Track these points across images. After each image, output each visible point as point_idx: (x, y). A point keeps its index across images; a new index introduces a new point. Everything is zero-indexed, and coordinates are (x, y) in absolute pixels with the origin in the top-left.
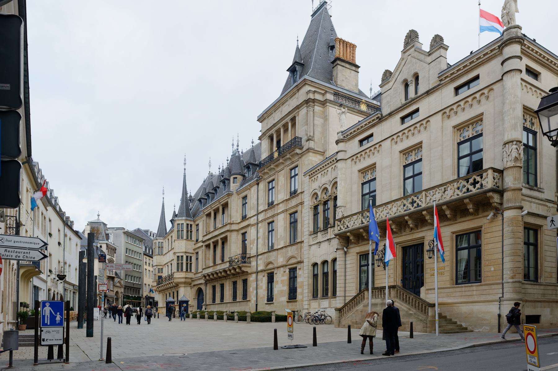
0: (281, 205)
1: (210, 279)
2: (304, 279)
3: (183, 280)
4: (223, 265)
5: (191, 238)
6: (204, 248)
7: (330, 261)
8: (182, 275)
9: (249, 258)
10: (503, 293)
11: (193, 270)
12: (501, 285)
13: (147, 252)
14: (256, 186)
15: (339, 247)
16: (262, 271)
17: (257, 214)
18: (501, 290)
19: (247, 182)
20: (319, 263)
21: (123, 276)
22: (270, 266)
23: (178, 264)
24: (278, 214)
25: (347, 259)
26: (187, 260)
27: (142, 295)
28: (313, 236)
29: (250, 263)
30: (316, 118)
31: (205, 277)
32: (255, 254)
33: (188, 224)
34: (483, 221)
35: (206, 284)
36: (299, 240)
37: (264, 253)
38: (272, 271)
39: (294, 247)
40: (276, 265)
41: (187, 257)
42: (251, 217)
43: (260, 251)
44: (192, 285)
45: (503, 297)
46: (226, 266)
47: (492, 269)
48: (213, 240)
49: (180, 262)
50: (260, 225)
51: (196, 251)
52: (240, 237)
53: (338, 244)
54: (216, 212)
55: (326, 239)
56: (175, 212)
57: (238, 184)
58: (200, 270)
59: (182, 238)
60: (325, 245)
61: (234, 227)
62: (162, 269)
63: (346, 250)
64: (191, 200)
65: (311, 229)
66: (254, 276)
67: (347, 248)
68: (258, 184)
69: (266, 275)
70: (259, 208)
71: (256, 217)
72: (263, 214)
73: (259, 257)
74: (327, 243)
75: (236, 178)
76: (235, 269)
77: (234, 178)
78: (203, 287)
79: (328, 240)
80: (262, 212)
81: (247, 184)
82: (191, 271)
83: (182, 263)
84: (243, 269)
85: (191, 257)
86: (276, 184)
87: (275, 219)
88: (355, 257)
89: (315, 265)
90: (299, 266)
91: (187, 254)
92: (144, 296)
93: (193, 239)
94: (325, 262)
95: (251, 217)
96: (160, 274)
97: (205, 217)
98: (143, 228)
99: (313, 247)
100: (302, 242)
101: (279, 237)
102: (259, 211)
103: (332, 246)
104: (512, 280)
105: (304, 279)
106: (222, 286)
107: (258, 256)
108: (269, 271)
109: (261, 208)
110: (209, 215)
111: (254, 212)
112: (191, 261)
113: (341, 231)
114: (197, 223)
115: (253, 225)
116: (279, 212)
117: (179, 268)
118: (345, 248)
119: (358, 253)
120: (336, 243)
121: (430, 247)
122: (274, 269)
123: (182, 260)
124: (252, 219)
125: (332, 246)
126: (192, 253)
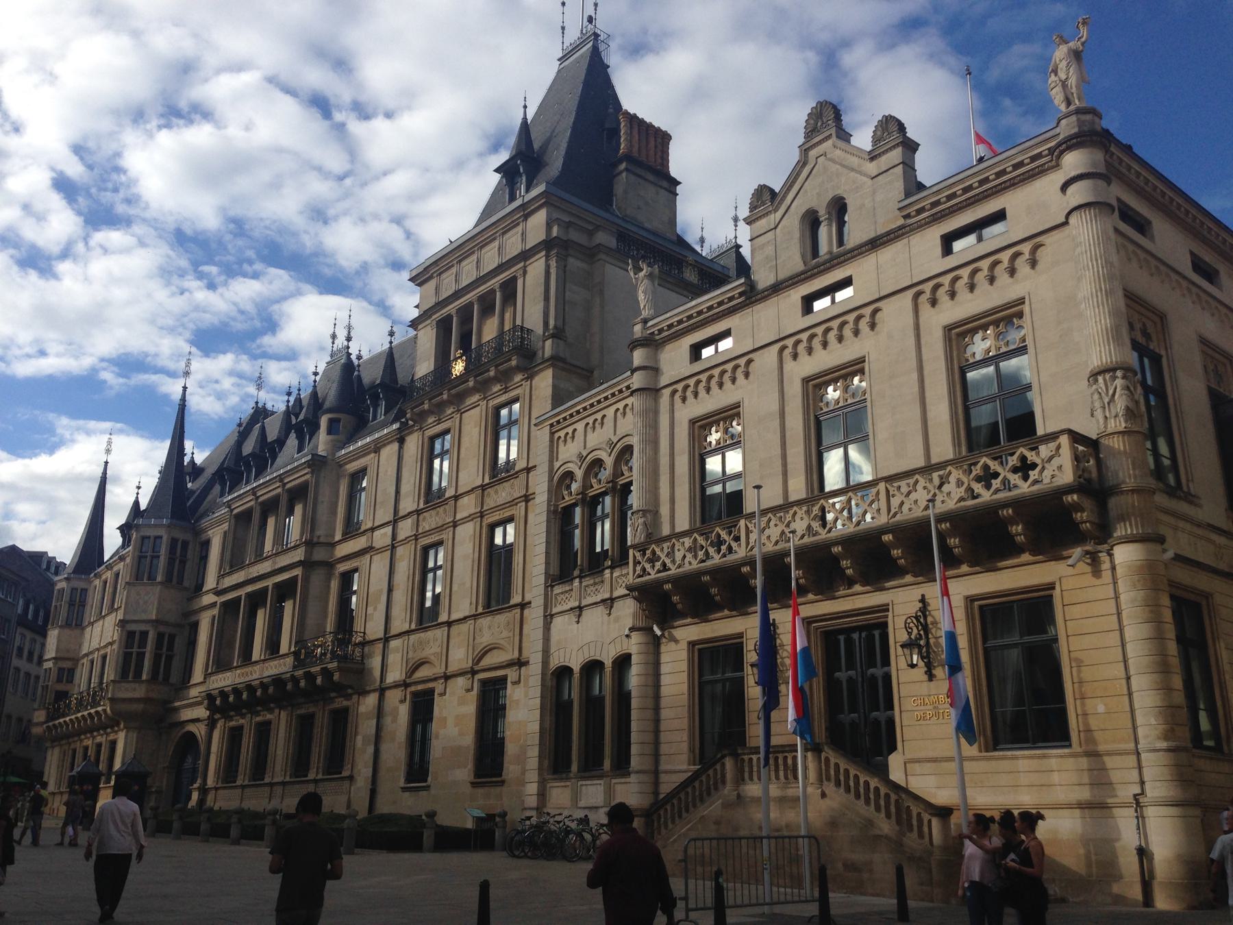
2: (524, 711)
3: (139, 707)
4: (273, 663)
5: (180, 581)
6: (215, 611)
7: (608, 663)
9: (364, 644)
10: (1142, 783)
11: (174, 678)
12: (1134, 757)
14: (396, 446)
15: (640, 624)
16: (396, 686)
17: (395, 522)
18: (1135, 775)
19: (370, 434)
20: (576, 667)
22: (422, 673)
23: (127, 657)
24: (455, 524)
25: (664, 658)
28: (558, 590)
30: (568, 285)
31: (210, 697)
32: (382, 635)
33: (173, 542)
34: (1065, 576)
36: (516, 599)
38: (431, 685)
39: (502, 619)
40: (439, 670)
41: (160, 636)
42: (373, 529)
45: (1143, 793)
47: (1101, 708)
48: (249, 589)
50: (400, 551)
51: (193, 619)
52: (335, 585)
53: (635, 616)
55: (599, 598)
56: (137, 503)
57: (342, 437)
58: (197, 676)
59: (152, 578)
60: (595, 617)
61: (319, 555)
62: (71, 672)
63: (659, 633)
64: (196, 471)
65: (554, 570)
66: (371, 700)
67: (662, 629)
68: (401, 441)
71: (389, 529)
72: (409, 521)
74: (601, 609)
75: (338, 420)
76: (310, 677)
77: (331, 421)
78: (200, 730)
79: (603, 601)
80: (409, 514)
81: (368, 440)
83: (141, 656)
84: (336, 677)
85: (172, 638)
86: (452, 445)
87: (446, 535)
88: (684, 655)
89: (564, 672)
90: (511, 674)
91: (162, 629)
93: (186, 584)
94: (593, 667)
99: (558, 622)
100: (523, 606)
102: (401, 513)
103: (617, 620)
104: (1164, 745)
105: (524, 711)
106: (264, 731)
107: (386, 639)
108: (420, 687)
109: (407, 505)
110: (243, 519)
111: (385, 515)
112: (171, 647)
113: (648, 578)
114: (204, 537)
116: (458, 517)
117: (129, 666)
118: (655, 628)
119: (692, 644)
120: (627, 610)
121: (910, 634)
122: (435, 679)
123: (143, 644)
124: (377, 533)
125: (617, 620)
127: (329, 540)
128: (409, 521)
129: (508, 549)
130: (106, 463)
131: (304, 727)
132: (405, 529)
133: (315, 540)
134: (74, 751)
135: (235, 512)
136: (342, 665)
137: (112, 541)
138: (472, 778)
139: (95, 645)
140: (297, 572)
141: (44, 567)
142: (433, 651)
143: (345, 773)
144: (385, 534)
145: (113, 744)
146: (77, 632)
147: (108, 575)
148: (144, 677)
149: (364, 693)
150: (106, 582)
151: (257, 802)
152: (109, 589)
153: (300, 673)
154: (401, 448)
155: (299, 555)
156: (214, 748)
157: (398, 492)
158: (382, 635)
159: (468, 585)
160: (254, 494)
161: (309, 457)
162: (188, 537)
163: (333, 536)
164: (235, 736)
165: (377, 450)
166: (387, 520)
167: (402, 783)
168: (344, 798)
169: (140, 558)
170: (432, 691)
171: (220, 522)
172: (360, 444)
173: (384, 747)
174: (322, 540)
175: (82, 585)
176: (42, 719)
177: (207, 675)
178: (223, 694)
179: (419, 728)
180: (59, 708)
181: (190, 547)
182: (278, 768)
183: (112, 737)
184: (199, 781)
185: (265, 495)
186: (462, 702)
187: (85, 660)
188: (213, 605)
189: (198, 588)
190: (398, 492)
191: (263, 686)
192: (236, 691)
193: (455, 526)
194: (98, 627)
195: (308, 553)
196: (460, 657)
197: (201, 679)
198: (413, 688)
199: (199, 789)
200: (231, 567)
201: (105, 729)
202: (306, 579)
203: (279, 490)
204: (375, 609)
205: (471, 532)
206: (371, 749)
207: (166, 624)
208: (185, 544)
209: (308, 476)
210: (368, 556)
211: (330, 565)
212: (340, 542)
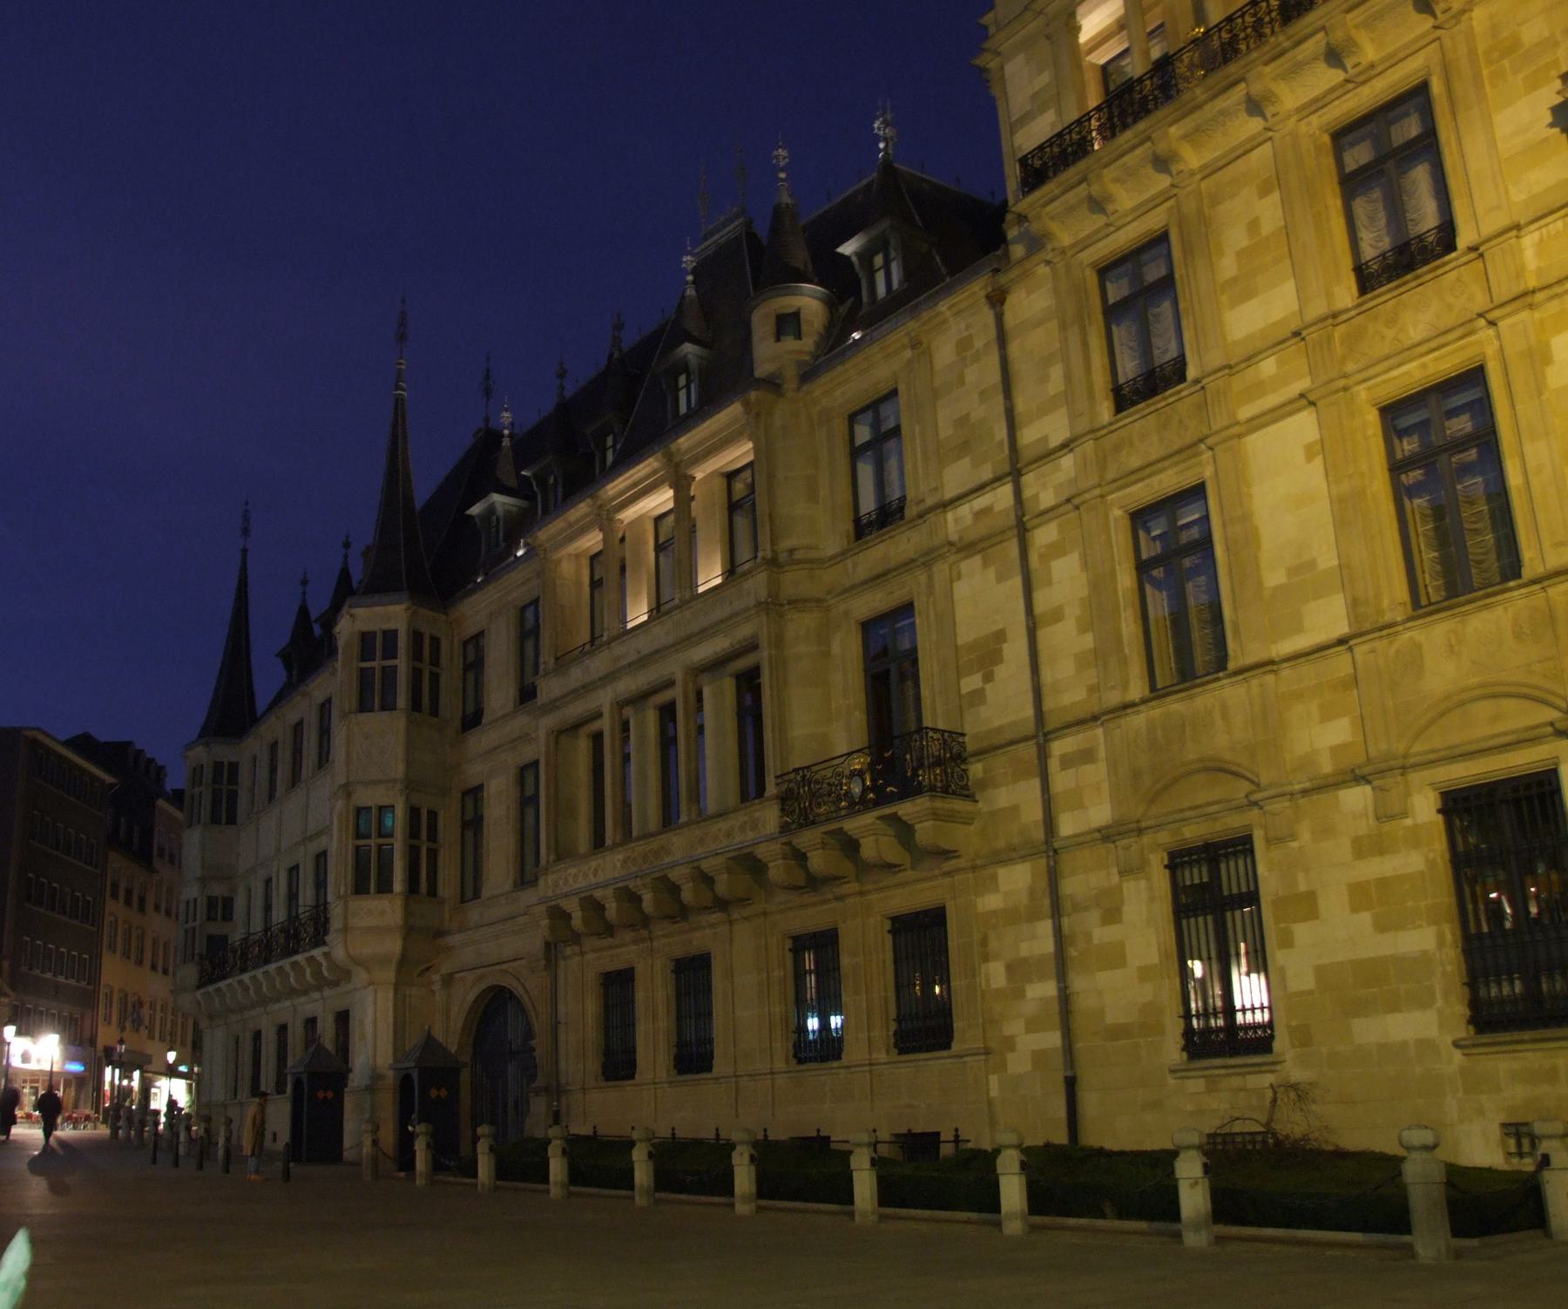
17: (1015, 472)
29: (966, 792)
41: (414, 813)
42: (945, 505)
49: (373, 842)
50: (1044, 536)
62: (228, 903)
66: (1018, 879)
70: (1028, 436)
71: (1005, 493)
78: (529, 986)
80: (1066, 446)
85: (433, 815)
96: (216, 929)
101: (1274, 578)
127: (814, 554)
128: (1067, 462)
130: (245, 551)
132: (1043, 489)
134: (257, 1035)
137: (267, 676)
138: (1463, 1031)
144: (986, 511)
148: (398, 886)
153: (806, 839)
154: (999, 319)
158: (1030, 728)
159: (1327, 559)
166: (986, 473)
174: (799, 555)
184: (540, 1081)
186: (1368, 847)
188: (524, 738)
196: (1323, 737)
198: (1164, 837)
201: (319, 988)
204: (988, 678)
205: (1312, 434)
206: (1049, 989)
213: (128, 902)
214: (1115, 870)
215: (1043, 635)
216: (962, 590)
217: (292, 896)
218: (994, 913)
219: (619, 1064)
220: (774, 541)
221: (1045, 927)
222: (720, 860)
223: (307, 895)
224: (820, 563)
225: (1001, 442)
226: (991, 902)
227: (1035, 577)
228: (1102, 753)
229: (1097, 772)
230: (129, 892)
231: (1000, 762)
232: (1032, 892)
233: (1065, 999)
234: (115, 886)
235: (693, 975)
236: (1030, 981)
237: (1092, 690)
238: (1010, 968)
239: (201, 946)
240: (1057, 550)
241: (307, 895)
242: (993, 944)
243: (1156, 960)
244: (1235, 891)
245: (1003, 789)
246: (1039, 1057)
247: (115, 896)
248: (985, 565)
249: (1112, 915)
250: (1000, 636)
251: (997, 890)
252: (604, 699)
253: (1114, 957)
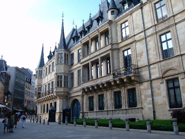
0: (179, 15)
1: (85, 91)
6: (81, 68)
8: (62, 90)
9: (138, 68)
11: (69, 86)
13: (27, 80)
14: (140, 10)
21: (13, 94)
23: (58, 82)
24: (176, 24)
26: (65, 79)
27: (23, 106)
31: (84, 89)
32: (147, 64)
33: (65, 54)
35: (83, 96)
37: (160, 61)
41: (65, 76)
42: (135, 36)
43: (152, 60)
44: (68, 97)
46: (110, 78)
49: (60, 80)
50: (148, 39)
51: (72, 72)
54: (96, 39)
56: (56, 46)
57: (115, 15)
61: (115, 47)
66: (146, 85)
68: (142, 8)
69: (165, 81)
71: (143, 34)
73: (152, 67)
76: (121, 80)
78: (79, 99)
80: (151, 27)
82: (67, 86)
83: (61, 81)
84: (133, 78)
85: (67, 77)
87: (170, 29)
91: (65, 75)
92: (24, 106)
93: (69, 64)
95: (135, 36)
96: (39, 92)
97: (82, 45)
98: (25, 68)
102: (146, 28)
107: (149, 65)
108: (170, 78)
109: (148, 25)
114: (72, 52)
115: (139, 41)
117: (59, 84)
123: (61, 78)
126: (69, 74)
128: (151, 29)
129: (129, 56)
131: (117, 95)
132: (149, 33)
133: (113, 43)
135: (82, 43)
136: (134, 74)
137: (46, 60)
139: (45, 82)
140: (110, 52)
141: (28, 71)
142: (174, 65)
143: (139, 106)
144: (140, 36)
145: (55, 103)
146: (41, 79)
147: (48, 66)
148: (63, 86)
149: (141, 83)
150: (47, 68)
151: (102, 116)
152: (48, 69)
153: (117, 79)
154: (142, 11)
155: (109, 47)
156: (84, 102)
157: (144, 23)
158: (147, 64)
160: (89, 37)
161: (108, 21)
162: (68, 53)
163: (117, 41)
164: (91, 99)
165: (131, 14)
167: (169, 109)
168: (141, 114)
169: (58, 58)
170: (177, 78)
171: (76, 48)
172: (121, 16)
173: (155, 98)
174: (115, 43)
175: (41, 70)
176: (36, 98)
177: (79, 85)
178: (88, 88)
179: (172, 91)
180: (40, 96)
181: (69, 55)
182: (109, 106)
183: (55, 101)
184: (81, 111)
185: (92, 36)
187: (44, 85)
189: (72, 64)
190: (144, 23)
191: (103, 84)
192: (93, 87)
193: (175, 25)
194: (46, 78)
195: (112, 47)
197: (77, 86)
198: (166, 79)
199: (82, 113)
200: (83, 57)
202: (112, 54)
203: (98, 33)
206: (151, 99)
207: (66, 74)
208: (67, 55)
209: (108, 26)
210: (134, 44)
211: (119, 49)
212: (121, 42)
213: (28, 88)
214: (159, 83)
215: (149, 52)
216: (137, 46)
217: (49, 87)
218: (142, 89)
219: (91, 109)
220: (112, 40)
221: (150, 91)
222: (105, 82)
223: (51, 87)
224: (118, 44)
225: (142, 27)
226: (142, 87)
227: (148, 44)
228: (157, 67)
229: (157, 70)
230: (28, 87)
231: (143, 69)
232: (147, 85)
233: (153, 100)
234: (26, 87)
235: (101, 97)
236: (147, 98)
237: (155, 59)
238: (145, 96)
239: (37, 94)
240: (150, 41)
241: (51, 87)
242: (142, 93)
243: (165, 95)
244: (178, 85)
245: (143, 72)
246: (149, 108)
247: (26, 87)
248: (140, 43)
249: (159, 89)
250: (142, 52)
251: (143, 86)
252: (89, 61)
253: (160, 95)
